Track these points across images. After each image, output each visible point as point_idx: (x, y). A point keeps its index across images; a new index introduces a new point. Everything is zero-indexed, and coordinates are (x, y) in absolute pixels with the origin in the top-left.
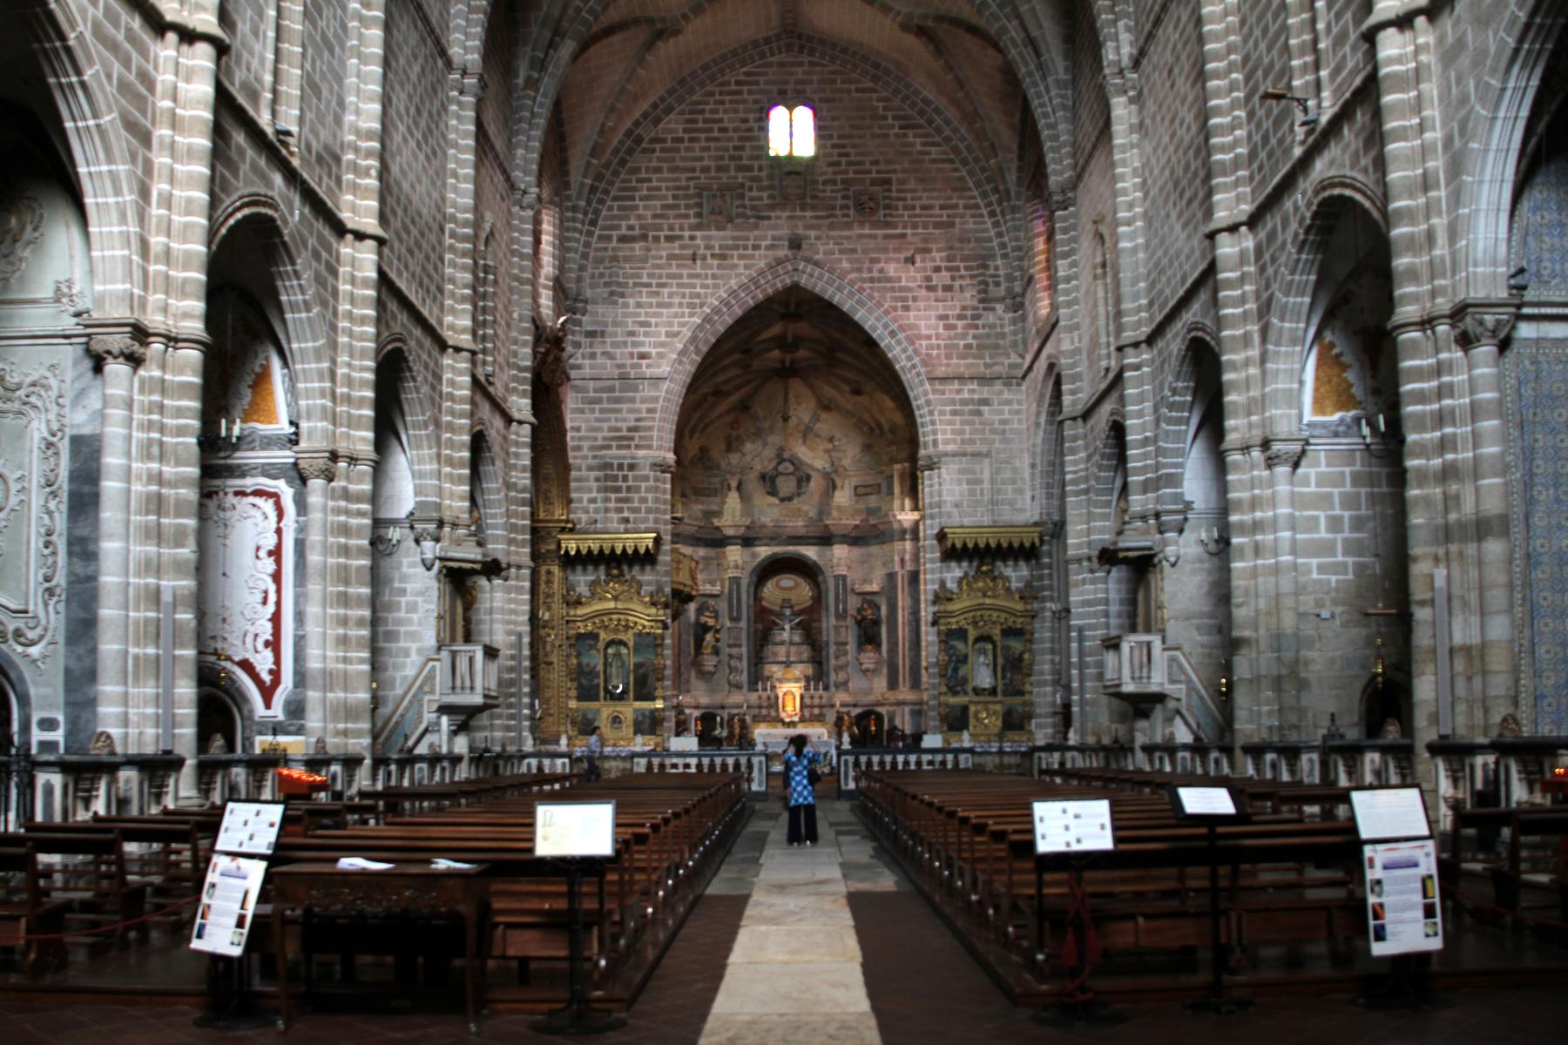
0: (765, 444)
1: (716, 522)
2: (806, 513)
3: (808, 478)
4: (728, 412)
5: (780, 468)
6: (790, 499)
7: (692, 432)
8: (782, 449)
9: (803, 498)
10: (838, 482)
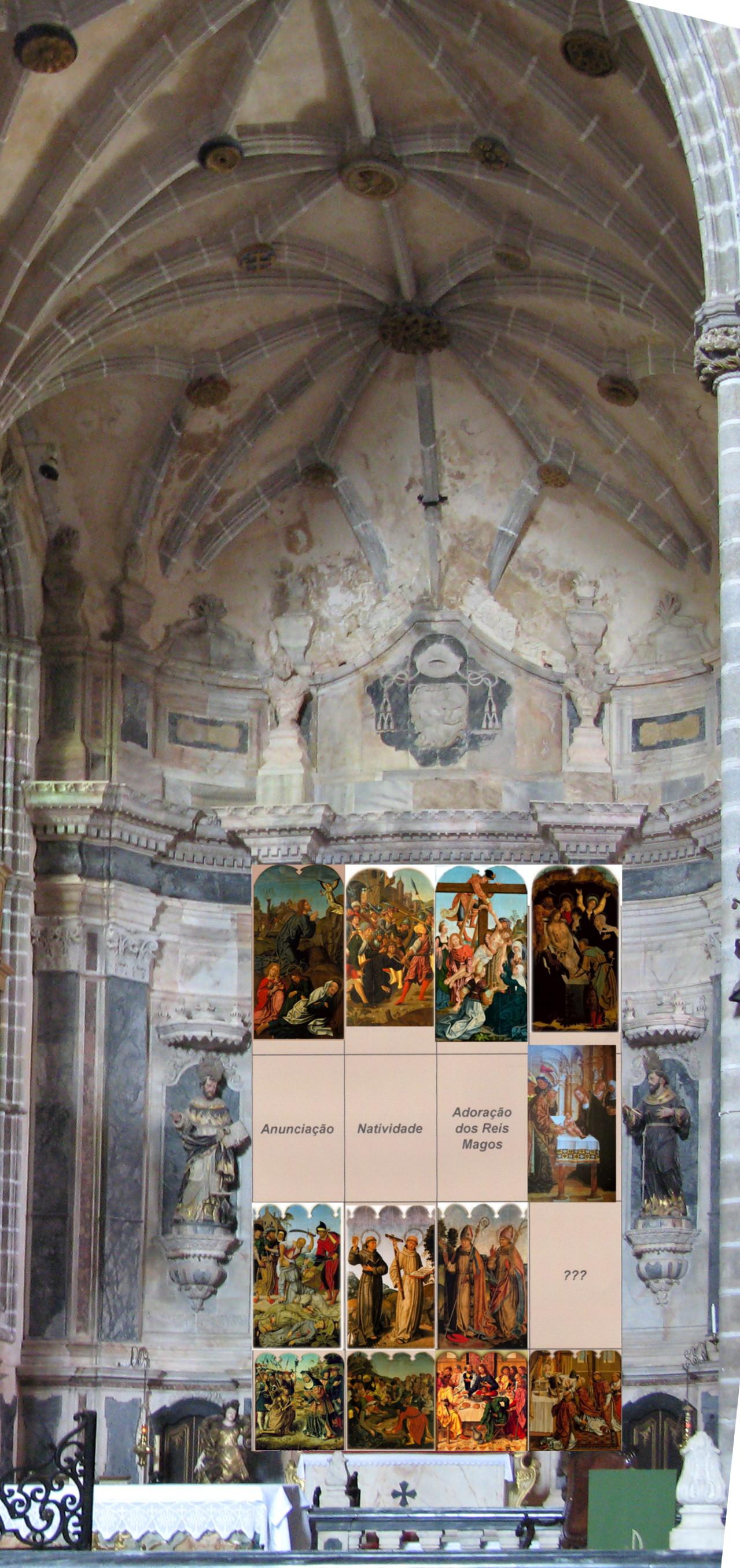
0: (381, 588)
1: (230, 820)
2: (493, 797)
3: (502, 691)
4: (273, 487)
5: (422, 661)
6: (448, 754)
7: (168, 546)
8: (426, 603)
9: (486, 752)
10: (586, 707)
